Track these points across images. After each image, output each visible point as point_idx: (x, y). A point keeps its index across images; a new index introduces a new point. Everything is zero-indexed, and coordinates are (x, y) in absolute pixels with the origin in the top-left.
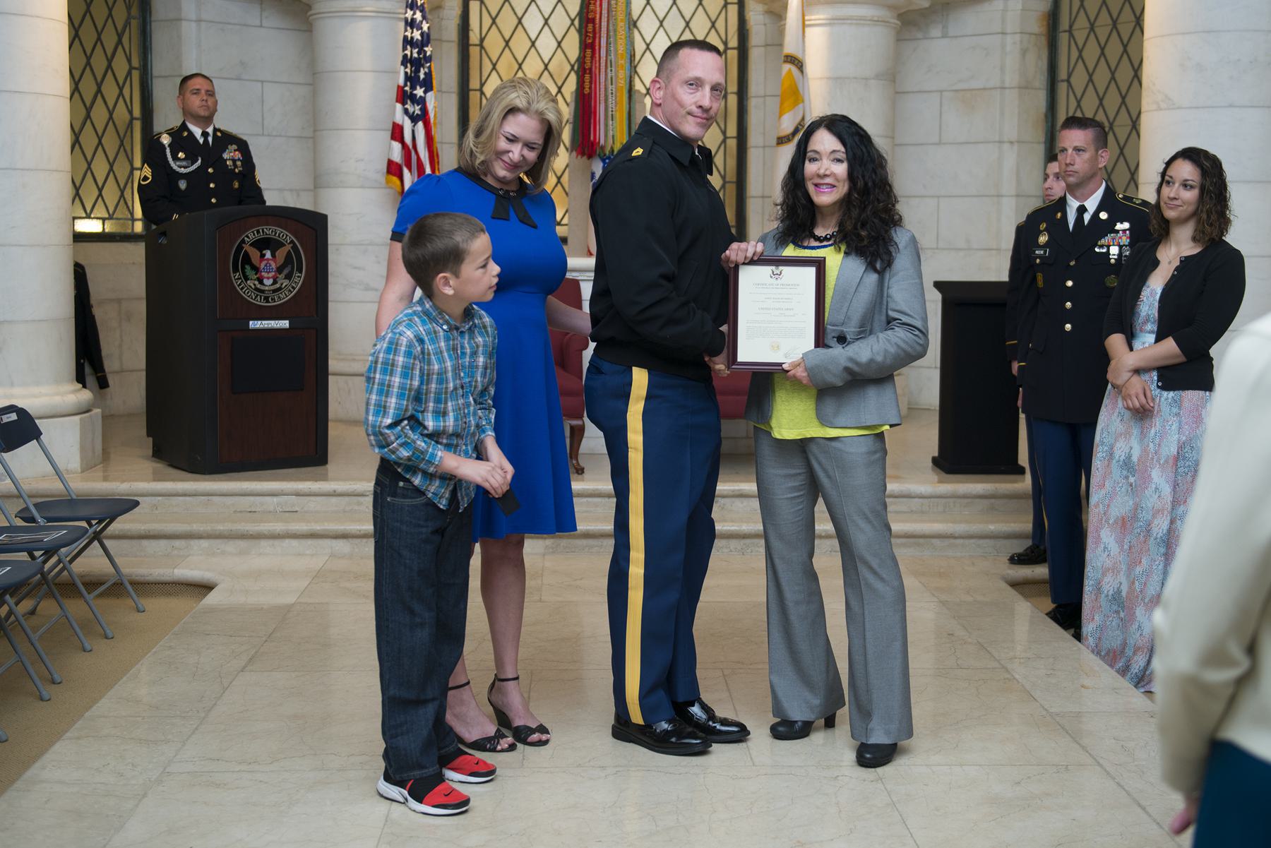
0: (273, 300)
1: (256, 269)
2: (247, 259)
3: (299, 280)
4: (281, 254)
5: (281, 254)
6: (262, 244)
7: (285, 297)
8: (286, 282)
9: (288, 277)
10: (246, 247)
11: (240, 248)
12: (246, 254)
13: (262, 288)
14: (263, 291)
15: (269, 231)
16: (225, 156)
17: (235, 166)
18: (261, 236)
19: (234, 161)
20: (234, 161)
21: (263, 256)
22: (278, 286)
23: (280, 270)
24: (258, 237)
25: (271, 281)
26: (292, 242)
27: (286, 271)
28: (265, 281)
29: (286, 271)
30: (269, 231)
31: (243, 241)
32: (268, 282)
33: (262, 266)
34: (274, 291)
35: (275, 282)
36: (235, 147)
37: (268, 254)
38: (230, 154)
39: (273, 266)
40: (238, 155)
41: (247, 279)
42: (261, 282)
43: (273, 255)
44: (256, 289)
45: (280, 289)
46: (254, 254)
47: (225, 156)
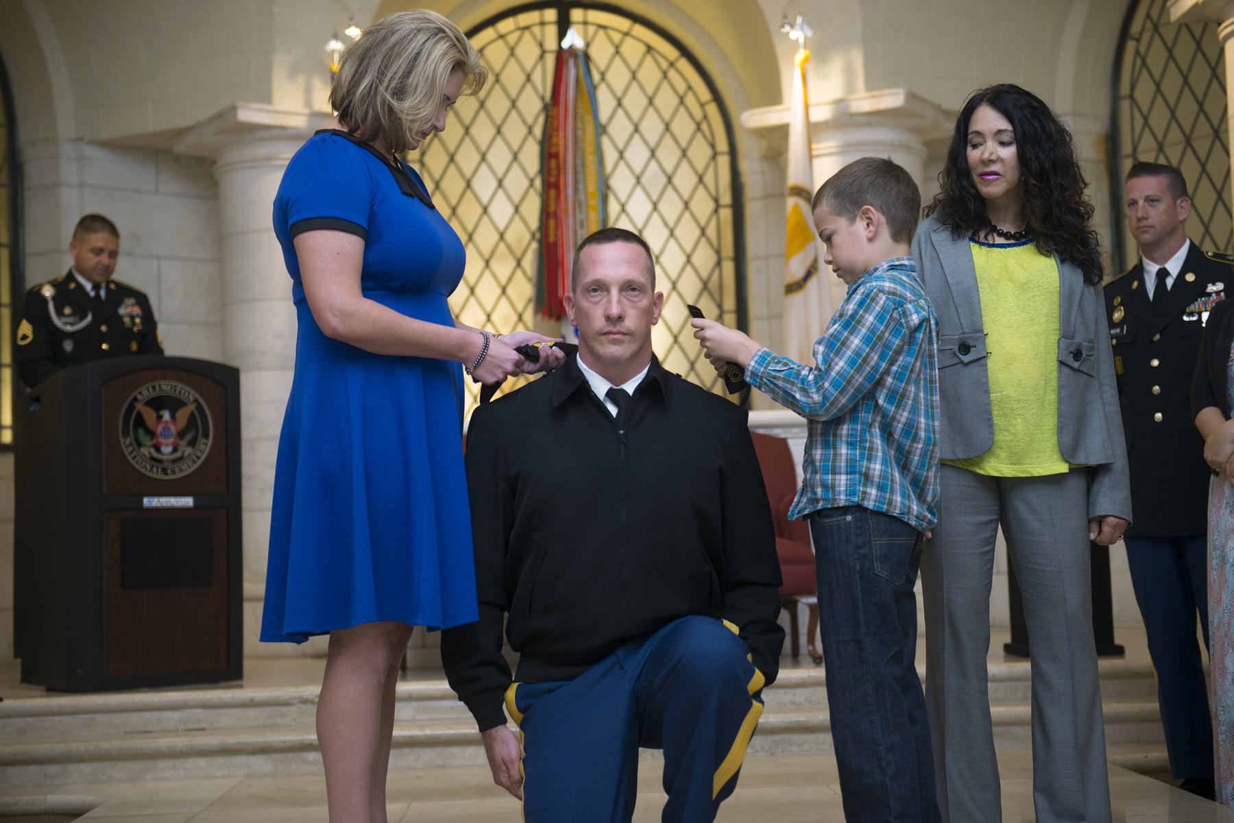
1: (151, 434)
2: (140, 422)
3: (205, 447)
4: (183, 415)
5: (183, 415)
6: (157, 403)
7: (187, 469)
8: (188, 451)
9: (192, 443)
10: (139, 407)
11: (131, 407)
14: (160, 461)
21: (160, 417)
22: (178, 454)
23: (181, 435)
24: (153, 394)
26: (196, 401)
27: (189, 437)
29: (189, 437)
30: (167, 387)
32: (167, 450)
34: (175, 461)
35: (175, 450)
37: (166, 415)
39: (173, 429)
41: (140, 445)
43: (173, 416)
44: (153, 459)
45: (181, 458)
46: (149, 415)
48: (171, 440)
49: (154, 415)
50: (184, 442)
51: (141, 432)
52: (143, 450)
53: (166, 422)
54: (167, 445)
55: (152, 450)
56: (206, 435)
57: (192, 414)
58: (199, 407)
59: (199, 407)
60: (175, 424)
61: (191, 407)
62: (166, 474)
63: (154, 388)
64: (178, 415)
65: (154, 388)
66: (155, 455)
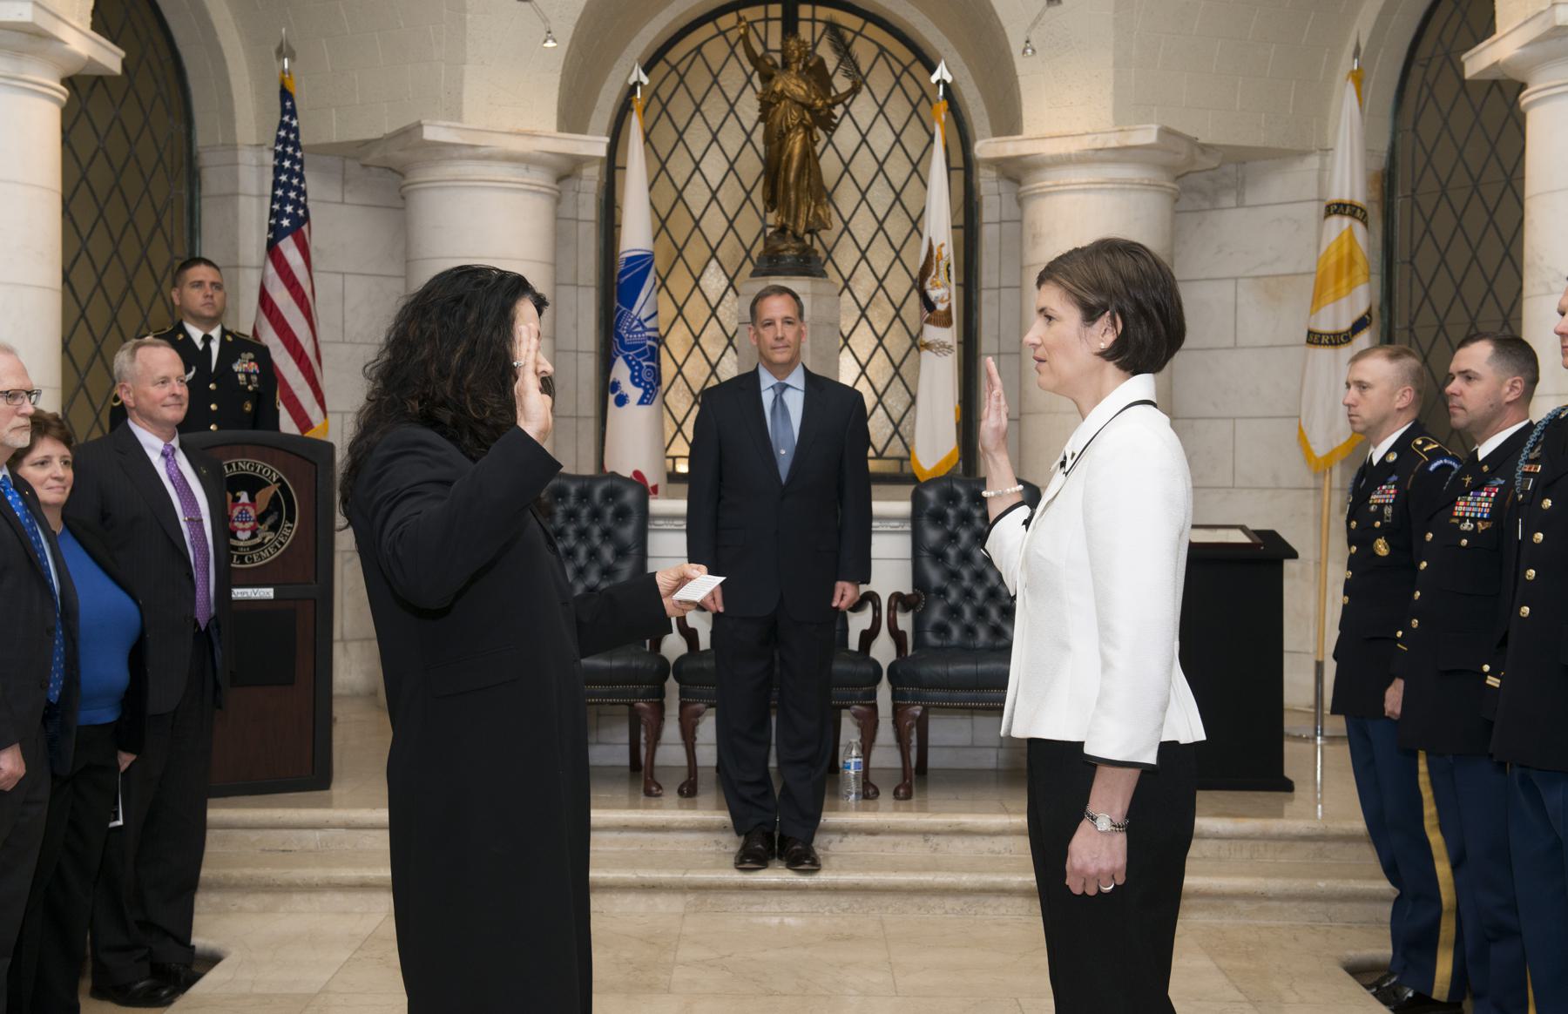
3: (289, 532)
9: (274, 528)
16: (237, 367)
17: (249, 382)
19: (248, 374)
20: (248, 374)
22: (258, 540)
23: (261, 519)
27: (270, 521)
28: (240, 535)
29: (270, 521)
33: (236, 512)
35: (254, 535)
36: (251, 355)
38: (244, 366)
40: (253, 367)
47: (237, 367)
48: (247, 525)
50: (265, 526)
56: (292, 521)
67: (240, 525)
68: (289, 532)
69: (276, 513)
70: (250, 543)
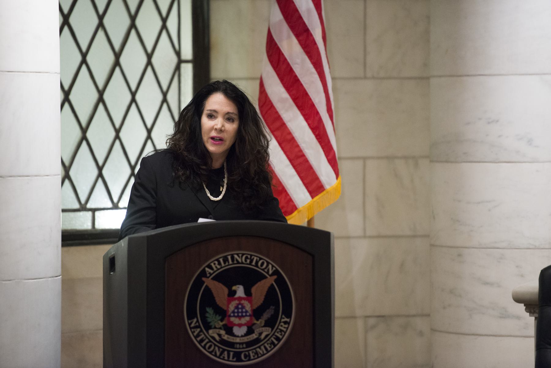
0: (248, 357)
1: (222, 313)
2: (209, 299)
3: (286, 327)
4: (260, 290)
5: (260, 290)
6: (228, 278)
8: (266, 331)
9: (271, 323)
10: (208, 282)
11: (199, 283)
12: (208, 290)
13: (231, 339)
14: (231, 345)
15: (240, 258)
18: (230, 264)
21: (232, 294)
22: (254, 336)
23: (257, 313)
25: (244, 330)
26: (276, 272)
27: (266, 315)
28: (237, 331)
29: (266, 315)
31: (203, 274)
32: (240, 331)
34: (249, 344)
35: (250, 331)
37: (240, 291)
39: (248, 307)
42: (229, 330)
43: (248, 292)
44: (223, 342)
45: (257, 341)
46: (220, 292)
48: (244, 320)
49: (226, 291)
50: (261, 322)
51: (210, 310)
52: (211, 331)
53: (240, 299)
54: (240, 325)
55: (223, 332)
56: (289, 316)
57: (272, 287)
58: (280, 281)
59: (280, 281)
60: (250, 302)
61: (271, 280)
62: (239, 360)
63: (226, 260)
64: (253, 290)
65: (226, 260)
66: (226, 337)
67: (236, 321)
68: (286, 327)
69: (272, 308)
70: (246, 339)
